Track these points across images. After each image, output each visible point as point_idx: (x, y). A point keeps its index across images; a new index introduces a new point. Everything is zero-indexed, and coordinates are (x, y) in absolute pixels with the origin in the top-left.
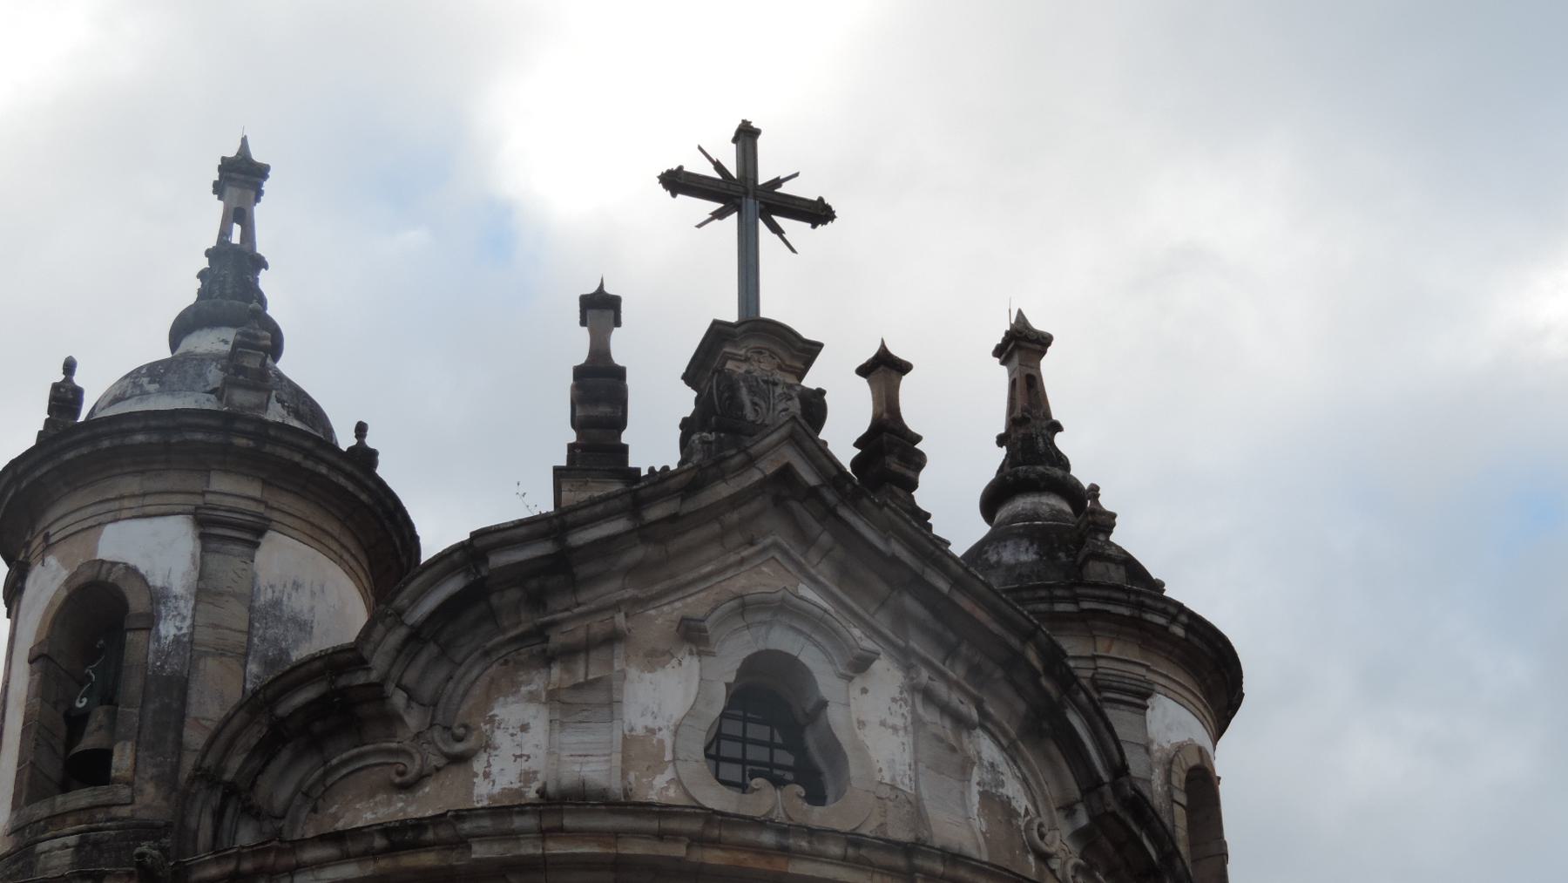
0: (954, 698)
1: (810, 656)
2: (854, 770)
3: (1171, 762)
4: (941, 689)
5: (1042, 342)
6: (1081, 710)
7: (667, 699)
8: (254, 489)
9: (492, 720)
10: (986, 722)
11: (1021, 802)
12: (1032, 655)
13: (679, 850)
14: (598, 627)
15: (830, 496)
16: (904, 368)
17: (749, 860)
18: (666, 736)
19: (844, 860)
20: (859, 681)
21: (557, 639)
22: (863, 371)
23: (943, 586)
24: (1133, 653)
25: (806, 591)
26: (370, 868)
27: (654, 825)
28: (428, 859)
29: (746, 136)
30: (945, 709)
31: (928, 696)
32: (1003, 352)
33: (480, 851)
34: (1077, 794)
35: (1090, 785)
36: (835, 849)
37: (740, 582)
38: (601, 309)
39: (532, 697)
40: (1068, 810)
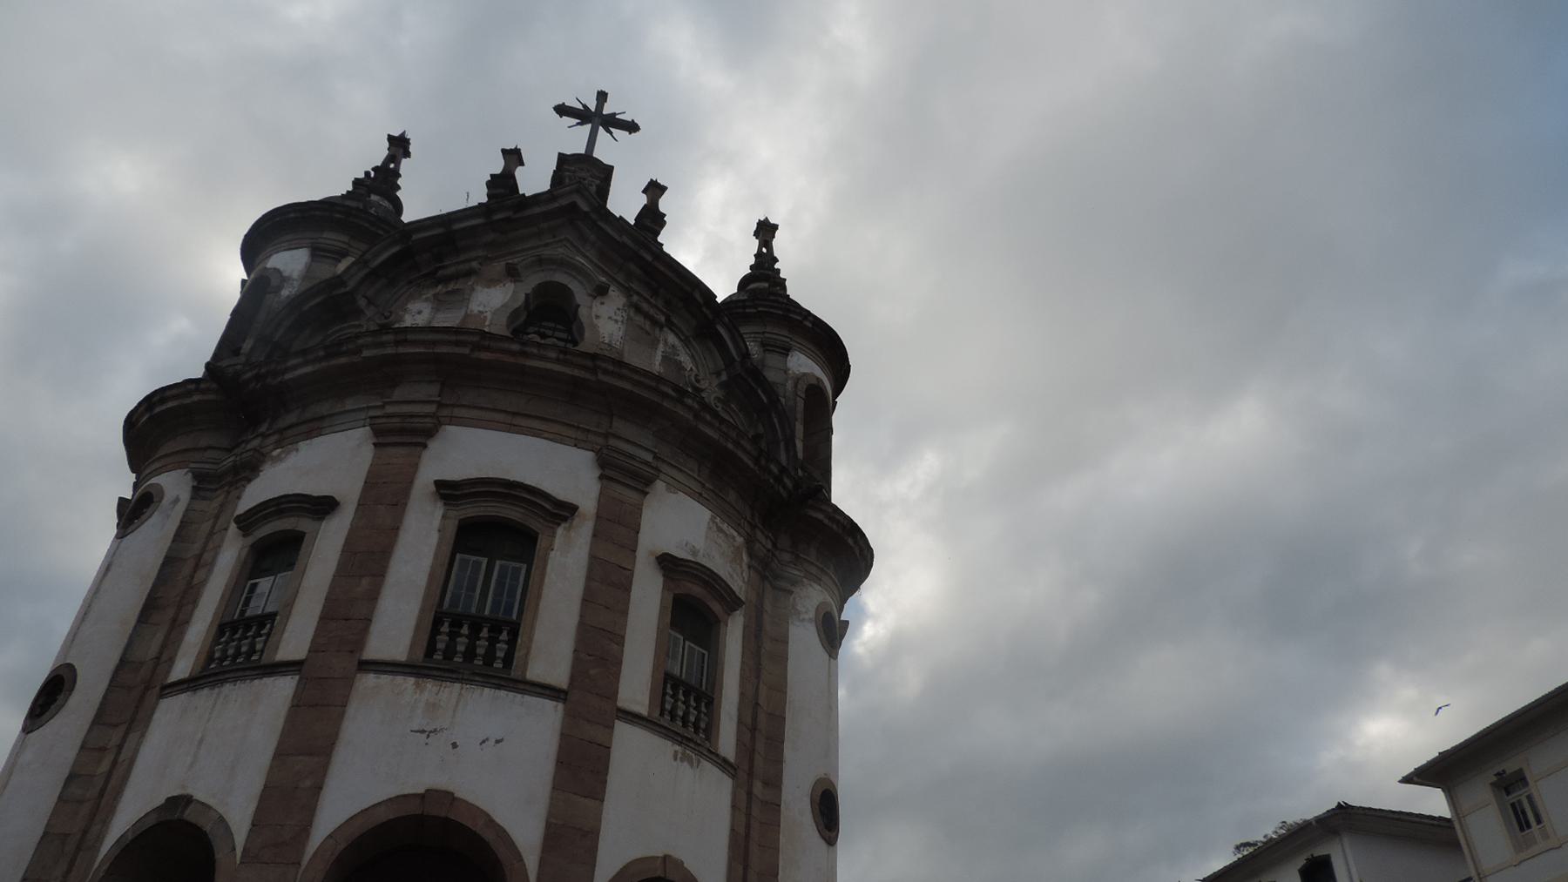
0: (652, 311)
1: (574, 286)
2: (587, 334)
4: (645, 306)
5: (775, 227)
8: (345, 239)
9: (405, 310)
10: (670, 324)
11: (688, 364)
12: (697, 296)
13: (466, 351)
15: (594, 216)
16: (663, 189)
18: (489, 315)
19: (558, 361)
20: (599, 299)
21: (440, 273)
22: (644, 191)
23: (649, 258)
26: (317, 366)
27: (453, 338)
28: (343, 360)
29: (602, 97)
30: (647, 316)
31: (638, 310)
32: (756, 234)
33: (366, 353)
35: (729, 363)
36: (553, 355)
38: (513, 157)
39: (427, 300)
40: (718, 374)
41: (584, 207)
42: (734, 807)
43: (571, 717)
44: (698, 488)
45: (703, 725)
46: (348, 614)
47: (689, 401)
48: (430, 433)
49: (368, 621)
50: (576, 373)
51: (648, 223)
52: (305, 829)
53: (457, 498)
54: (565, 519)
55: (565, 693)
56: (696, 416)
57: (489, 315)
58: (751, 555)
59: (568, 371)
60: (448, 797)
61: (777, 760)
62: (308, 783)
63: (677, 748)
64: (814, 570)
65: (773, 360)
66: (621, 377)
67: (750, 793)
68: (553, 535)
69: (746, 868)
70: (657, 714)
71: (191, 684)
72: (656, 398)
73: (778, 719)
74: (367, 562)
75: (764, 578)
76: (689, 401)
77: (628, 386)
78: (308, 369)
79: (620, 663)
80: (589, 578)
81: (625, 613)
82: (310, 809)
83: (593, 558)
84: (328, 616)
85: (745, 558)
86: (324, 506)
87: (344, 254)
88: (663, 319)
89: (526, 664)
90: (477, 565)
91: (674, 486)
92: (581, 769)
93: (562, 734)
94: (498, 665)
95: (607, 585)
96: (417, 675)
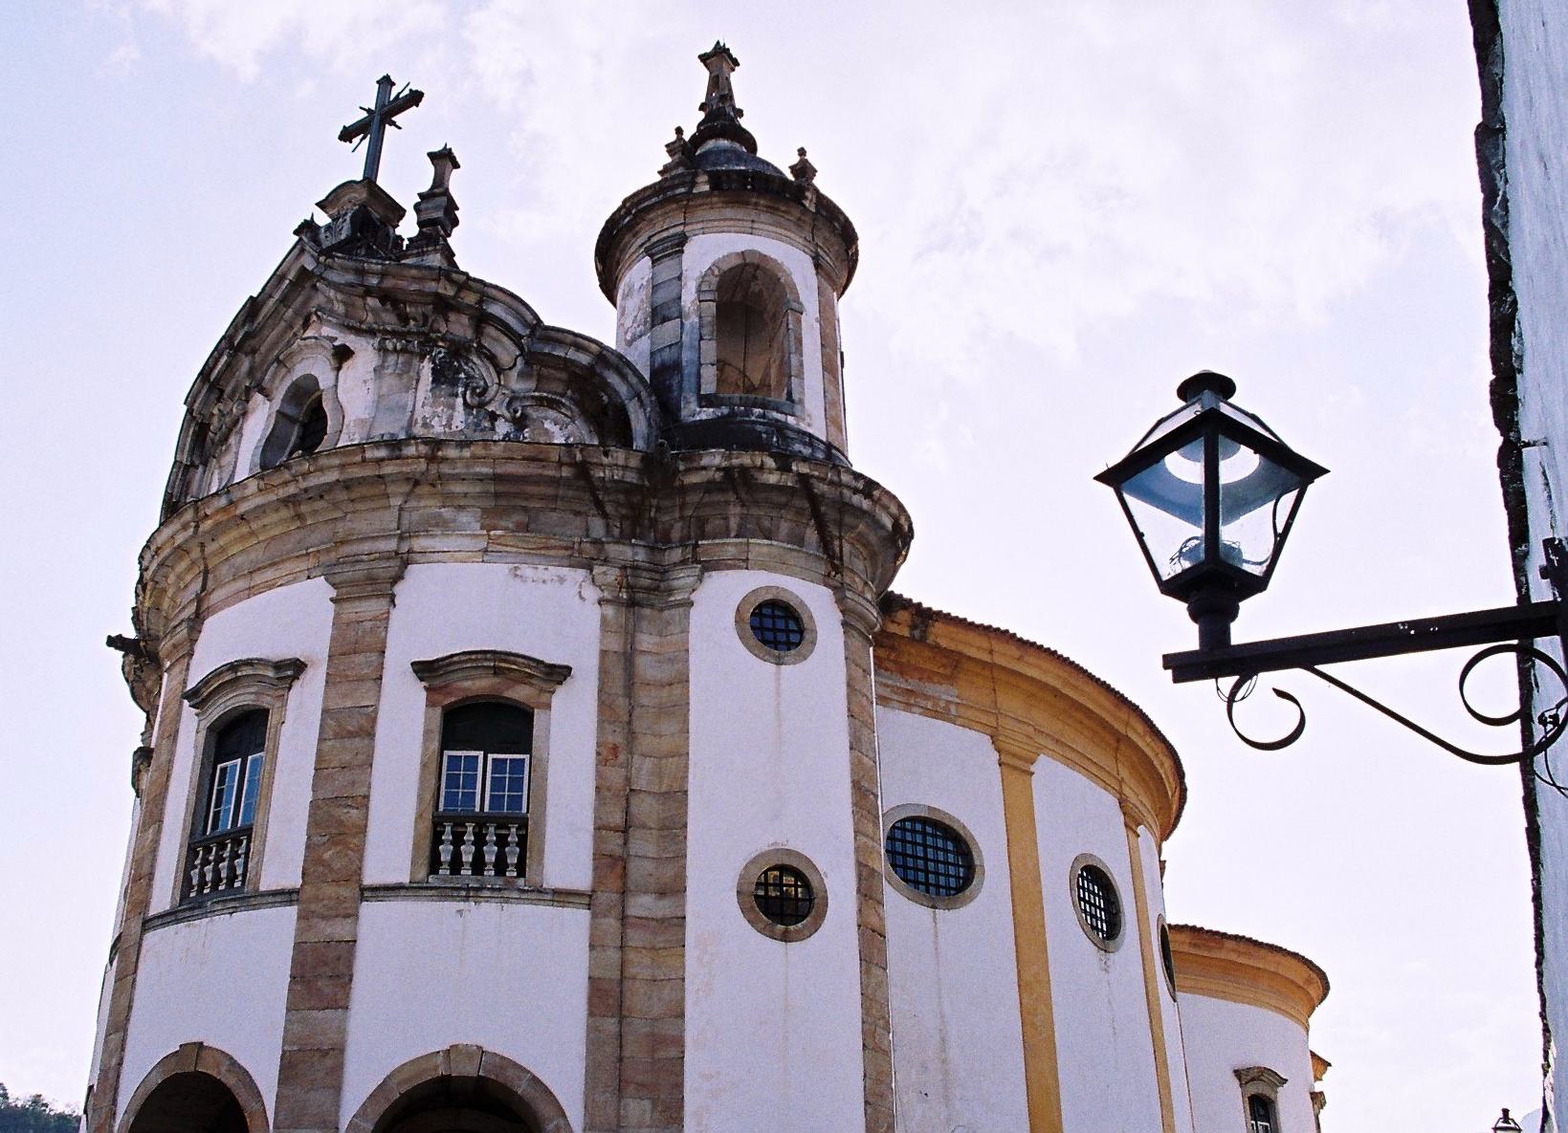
6: (495, 300)
23: (374, 281)
42: (592, 947)
45: (513, 860)
50: (282, 493)
53: (205, 701)
54: (295, 677)
55: (296, 891)
56: (432, 459)
59: (273, 497)
63: (462, 905)
66: (321, 470)
67: (623, 918)
68: (284, 705)
70: (422, 874)
72: (368, 472)
73: (677, 796)
75: (632, 604)
77: (332, 476)
79: (362, 830)
80: (321, 740)
83: (325, 711)
89: (258, 875)
92: (322, 976)
93: (297, 945)
96: (178, 921)
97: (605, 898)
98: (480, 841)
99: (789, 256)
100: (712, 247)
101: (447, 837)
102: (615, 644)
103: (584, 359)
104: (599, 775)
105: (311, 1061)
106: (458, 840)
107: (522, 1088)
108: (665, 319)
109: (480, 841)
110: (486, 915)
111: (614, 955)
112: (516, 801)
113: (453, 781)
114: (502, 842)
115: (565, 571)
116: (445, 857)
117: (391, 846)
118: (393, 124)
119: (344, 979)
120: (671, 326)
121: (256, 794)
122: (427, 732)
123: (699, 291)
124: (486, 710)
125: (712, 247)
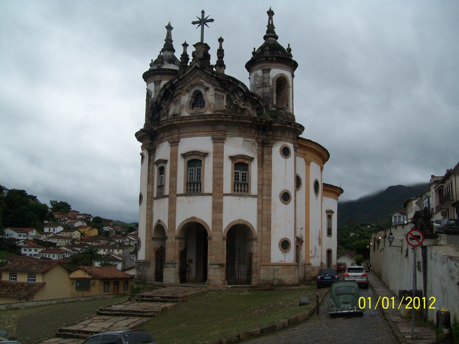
3: (274, 78)
6: (240, 84)
7: (186, 99)
8: (160, 76)
12: (231, 81)
13: (179, 122)
14: (177, 93)
17: (187, 121)
19: (197, 119)
23: (216, 75)
24: (269, 64)
25: (202, 81)
29: (203, 12)
30: (219, 91)
31: (216, 90)
34: (242, 94)
37: (194, 82)
41: (199, 66)
42: (258, 204)
43: (213, 198)
44: (239, 134)
46: (173, 186)
47: (229, 117)
48: (178, 142)
49: (176, 186)
50: (202, 120)
51: (219, 56)
52: (175, 226)
57: (185, 105)
58: (258, 143)
60: (194, 218)
61: (270, 190)
62: (173, 218)
64: (279, 138)
65: (266, 75)
67: (262, 199)
69: (262, 215)
70: (233, 192)
71: (157, 198)
72: (220, 119)
73: (270, 180)
74: (174, 173)
75: (263, 146)
76: (229, 117)
77: (213, 119)
78: (156, 128)
79: (223, 185)
80: (213, 168)
81: (222, 173)
82: (175, 223)
83: (214, 163)
84: (171, 186)
85: (256, 144)
86: (165, 162)
87: (160, 81)
88: (224, 90)
90: (193, 169)
91: (231, 136)
92: (218, 208)
93: (213, 203)
94: (199, 191)
95: (218, 167)
97: (260, 196)
98: (241, 187)
99: (287, 74)
100: (275, 72)
101: (236, 186)
102: (260, 153)
103: (256, 98)
104: (258, 176)
105: (217, 221)
106: (238, 187)
107: (249, 226)
108: (266, 87)
109: (241, 187)
110: (243, 199)
111: (261, 205)
112: (245, 180)
113: (235, 176)
114: (245, 187)
115: (252, 139)
116: (236, 189)
117: (227, 187)
118: (206, 25)
119: (221, 208)
120: (268, 88)
121: (199, 174)
122: (232, 168)
123: (273, 81)
124: (241, 164)
125: (275, 72)
